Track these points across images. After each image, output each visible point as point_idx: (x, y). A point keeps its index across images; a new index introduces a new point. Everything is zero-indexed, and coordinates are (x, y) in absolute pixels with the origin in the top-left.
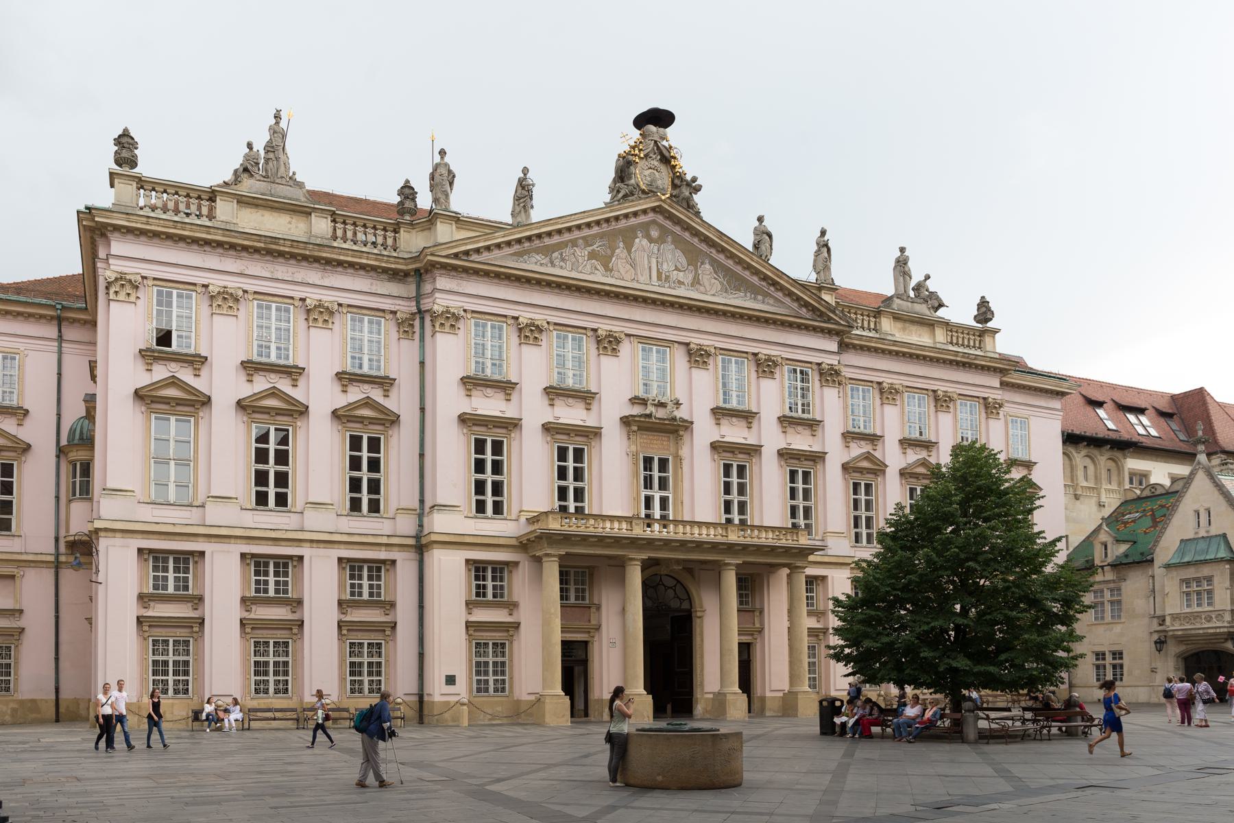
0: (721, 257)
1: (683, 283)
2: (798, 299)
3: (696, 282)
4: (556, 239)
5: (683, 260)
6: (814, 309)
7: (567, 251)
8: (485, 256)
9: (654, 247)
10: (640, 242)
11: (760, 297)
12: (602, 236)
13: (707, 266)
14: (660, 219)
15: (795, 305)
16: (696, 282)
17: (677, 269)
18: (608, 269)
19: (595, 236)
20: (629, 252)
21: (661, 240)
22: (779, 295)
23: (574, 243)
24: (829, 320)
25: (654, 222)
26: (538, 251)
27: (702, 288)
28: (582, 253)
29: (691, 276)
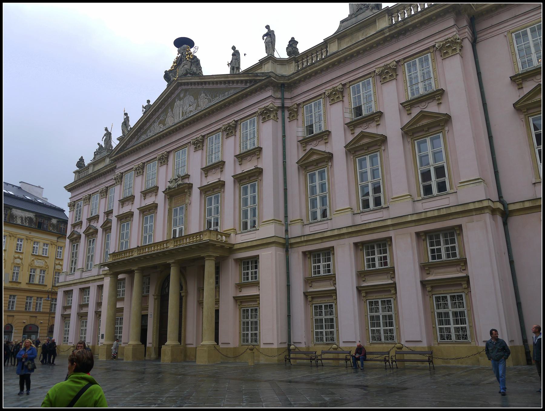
0: (207, 86)
1: (192, 111)
2: (242, 81)
3: (198, 106)
4: (148, 124)
5: (192, 99)
6: (251, 81)
7: (152, 127)
8: (128, 147)
9: (182, 101)
10: (178, 103)
11: (226, 93)
12: (162, 112)
13: (203, 95)
14: (183, 87)
15: (239, 85)
16: (198, 106)
17: (190, 106)
18: (164, 125)
19: (161, 113)
20: (172, 111)
21: (185, 96)
22: (235, 85)
23: (154, 122)
24: (256, 82)
25: (182, 90)
26: (142, 134)
27: (200, 108)
28: (156, 124)
29: (195, 105)
